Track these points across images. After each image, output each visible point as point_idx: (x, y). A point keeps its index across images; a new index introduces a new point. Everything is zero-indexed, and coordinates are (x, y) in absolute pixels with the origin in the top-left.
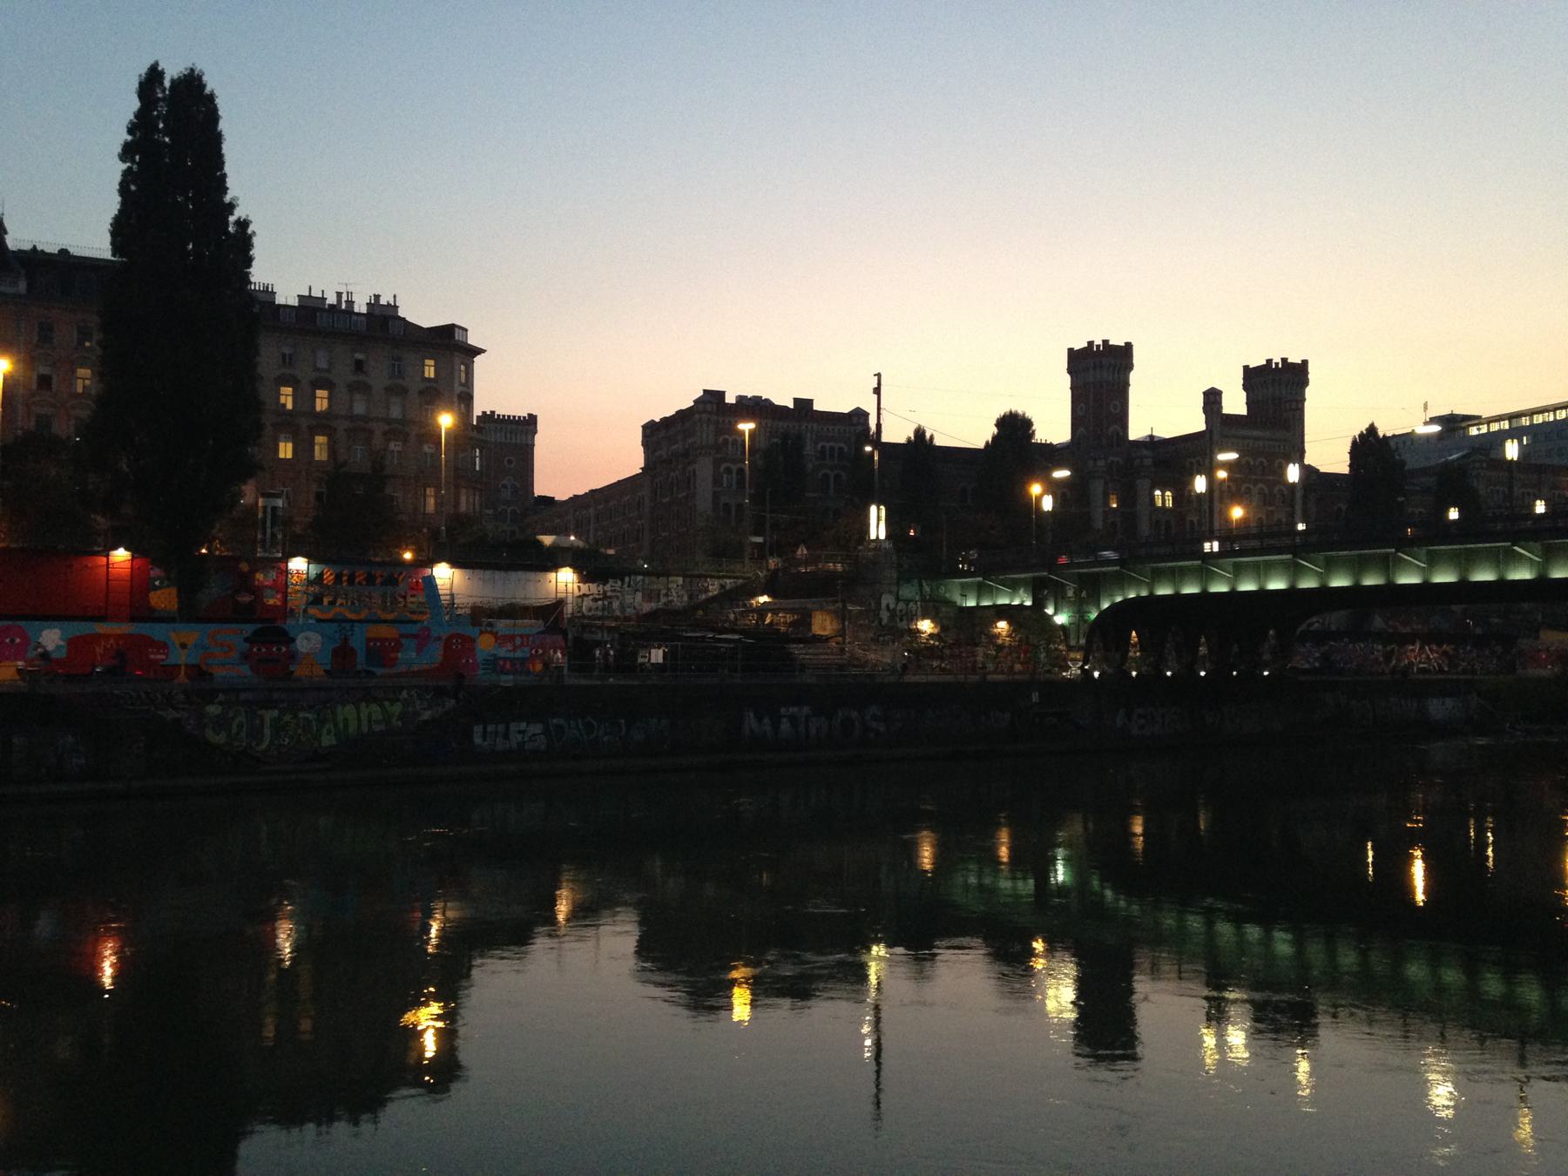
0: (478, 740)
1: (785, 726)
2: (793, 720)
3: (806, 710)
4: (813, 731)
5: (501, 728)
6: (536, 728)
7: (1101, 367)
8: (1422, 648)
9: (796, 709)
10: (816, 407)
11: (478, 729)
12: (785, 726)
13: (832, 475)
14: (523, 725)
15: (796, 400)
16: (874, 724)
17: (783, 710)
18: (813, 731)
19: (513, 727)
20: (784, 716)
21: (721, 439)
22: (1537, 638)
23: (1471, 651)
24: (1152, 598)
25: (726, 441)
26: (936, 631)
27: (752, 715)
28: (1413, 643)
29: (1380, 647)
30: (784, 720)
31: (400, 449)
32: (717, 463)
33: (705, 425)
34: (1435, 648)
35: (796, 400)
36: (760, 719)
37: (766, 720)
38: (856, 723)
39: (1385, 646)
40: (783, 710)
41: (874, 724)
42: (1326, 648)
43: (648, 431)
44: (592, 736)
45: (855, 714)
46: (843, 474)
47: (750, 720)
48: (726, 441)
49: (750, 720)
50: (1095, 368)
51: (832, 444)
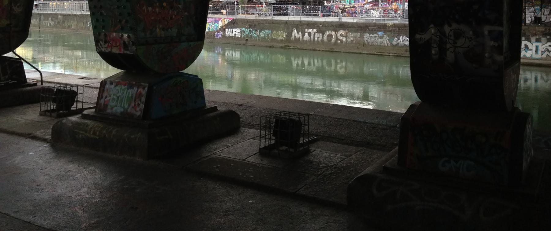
0: (226, 33)
1: (307, 35)
2: (310, 34)
3: (315, 30)
4: (316, 39)
5: (232, 30)
6: (239, 31)
9: (311, 30)
11: (227, 30)
12: (307, 35)
14: (236, 30)
16: (341, 38)
17: (306, 30)
18: (316, 39)
19: (234, 30)
20: (306, 32)
27: (296, 30)
30: (306, 34)
36: (298, 33)
37: (300, 33)
38: (333, 37)
40: (306, 30)
41: (341, 38)
44: (251, 34)
45: (333, 33)
47: (295, 31)
49: (295, 31)
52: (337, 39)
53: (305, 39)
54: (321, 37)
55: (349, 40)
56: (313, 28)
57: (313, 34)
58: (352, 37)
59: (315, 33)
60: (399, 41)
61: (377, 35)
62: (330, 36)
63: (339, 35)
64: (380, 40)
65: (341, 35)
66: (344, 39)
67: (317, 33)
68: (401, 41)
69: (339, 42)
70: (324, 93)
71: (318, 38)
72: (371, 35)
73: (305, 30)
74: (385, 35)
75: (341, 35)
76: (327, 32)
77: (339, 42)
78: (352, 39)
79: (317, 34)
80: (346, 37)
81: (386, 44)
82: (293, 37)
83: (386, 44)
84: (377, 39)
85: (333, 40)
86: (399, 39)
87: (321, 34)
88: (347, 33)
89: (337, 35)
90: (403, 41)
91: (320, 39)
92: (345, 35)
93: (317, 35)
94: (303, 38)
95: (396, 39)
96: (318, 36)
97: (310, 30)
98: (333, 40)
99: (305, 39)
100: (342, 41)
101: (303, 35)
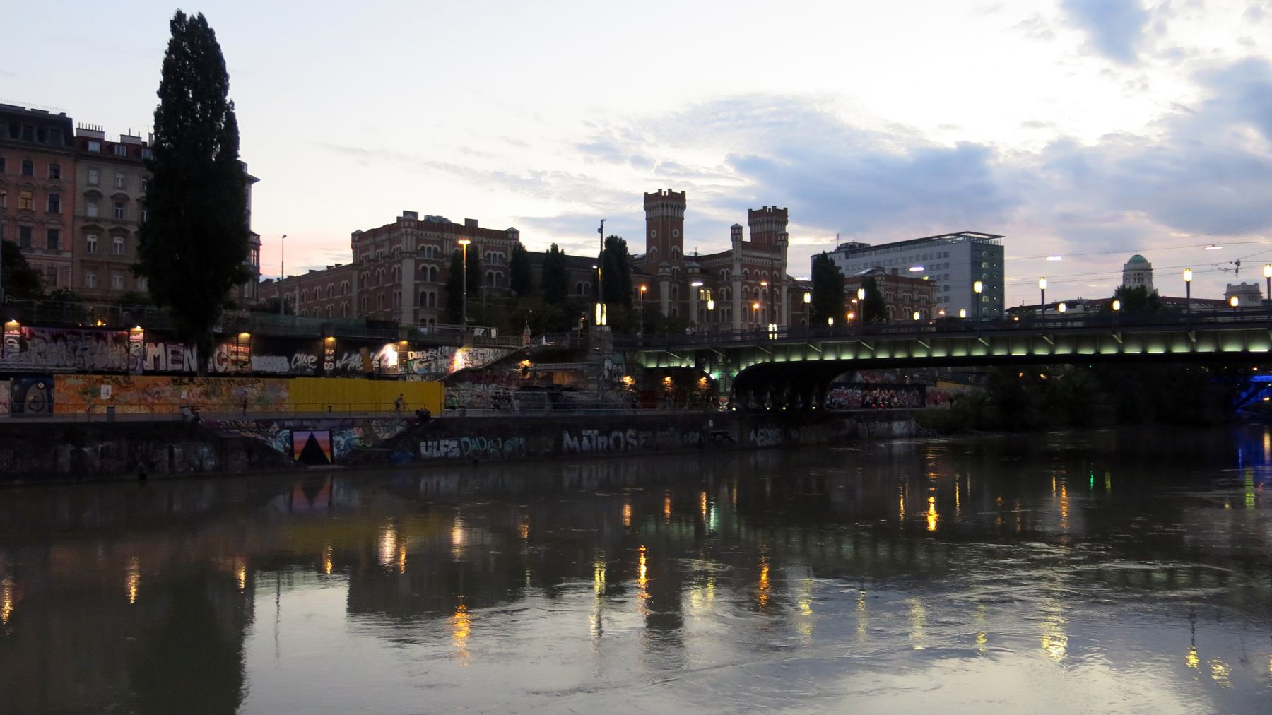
0: (423, 451)
1: (585, 441)
5: (436, 443)
6: (454, 444)
7: (667, 207)
8: (880, 392)
9: (591, 432)
10: (480, 225)
11: (423, 444)
12: (585, 441)
13: (495, 273)
14: (447, 442)
15: (466, 220)
18: (600, 445)
19: (442, 443)
21: (419, 248)
22: (936, 386)
23: (904, 394)
24: (774, 365)
25: (423, 248)
26: (633, 383)
27: (567, 434)
28: (876, 390)
29: (860, 392)
30: (585, 438)
31: (122, 242)
32: (417, 263)
33: (409, 237)
34: (887, 392)
35: (466, 220)
36: (572, 438)
37: (576, 439)
38: (622, 440)
39: (862, 391)
40: (584, 433)
42: (833, 392)
43: (357, 238)
44: (484, 449)
45: (621, 434)
46: (501, 272)
47: (567, 436)
48: (423, 248)
49: (567, 436)
50: (663, 206)
51: (495, 252)
52: (627, 443)
54: (606, 441)
55: (641, 443)
56: (592, 428)
57: (594, 438)
58: (643, 438)
62: (617, 440)
63: (628, 436)
65: (631, 436)
66: (635, 443)
71: (602, 444)
72: (663, 433)
75: (631, 436)
76: (613, 433)
78: (643, 441)
80: (637, 438)
82: (565, 446)
85: (622, 445)
86: (688, 436)
89: (625, 435)
91: (605, 446)
93: (600, 439)
96: (602, 441)
97: (590, 432)
100: (632, 445)
101: (580, 442)
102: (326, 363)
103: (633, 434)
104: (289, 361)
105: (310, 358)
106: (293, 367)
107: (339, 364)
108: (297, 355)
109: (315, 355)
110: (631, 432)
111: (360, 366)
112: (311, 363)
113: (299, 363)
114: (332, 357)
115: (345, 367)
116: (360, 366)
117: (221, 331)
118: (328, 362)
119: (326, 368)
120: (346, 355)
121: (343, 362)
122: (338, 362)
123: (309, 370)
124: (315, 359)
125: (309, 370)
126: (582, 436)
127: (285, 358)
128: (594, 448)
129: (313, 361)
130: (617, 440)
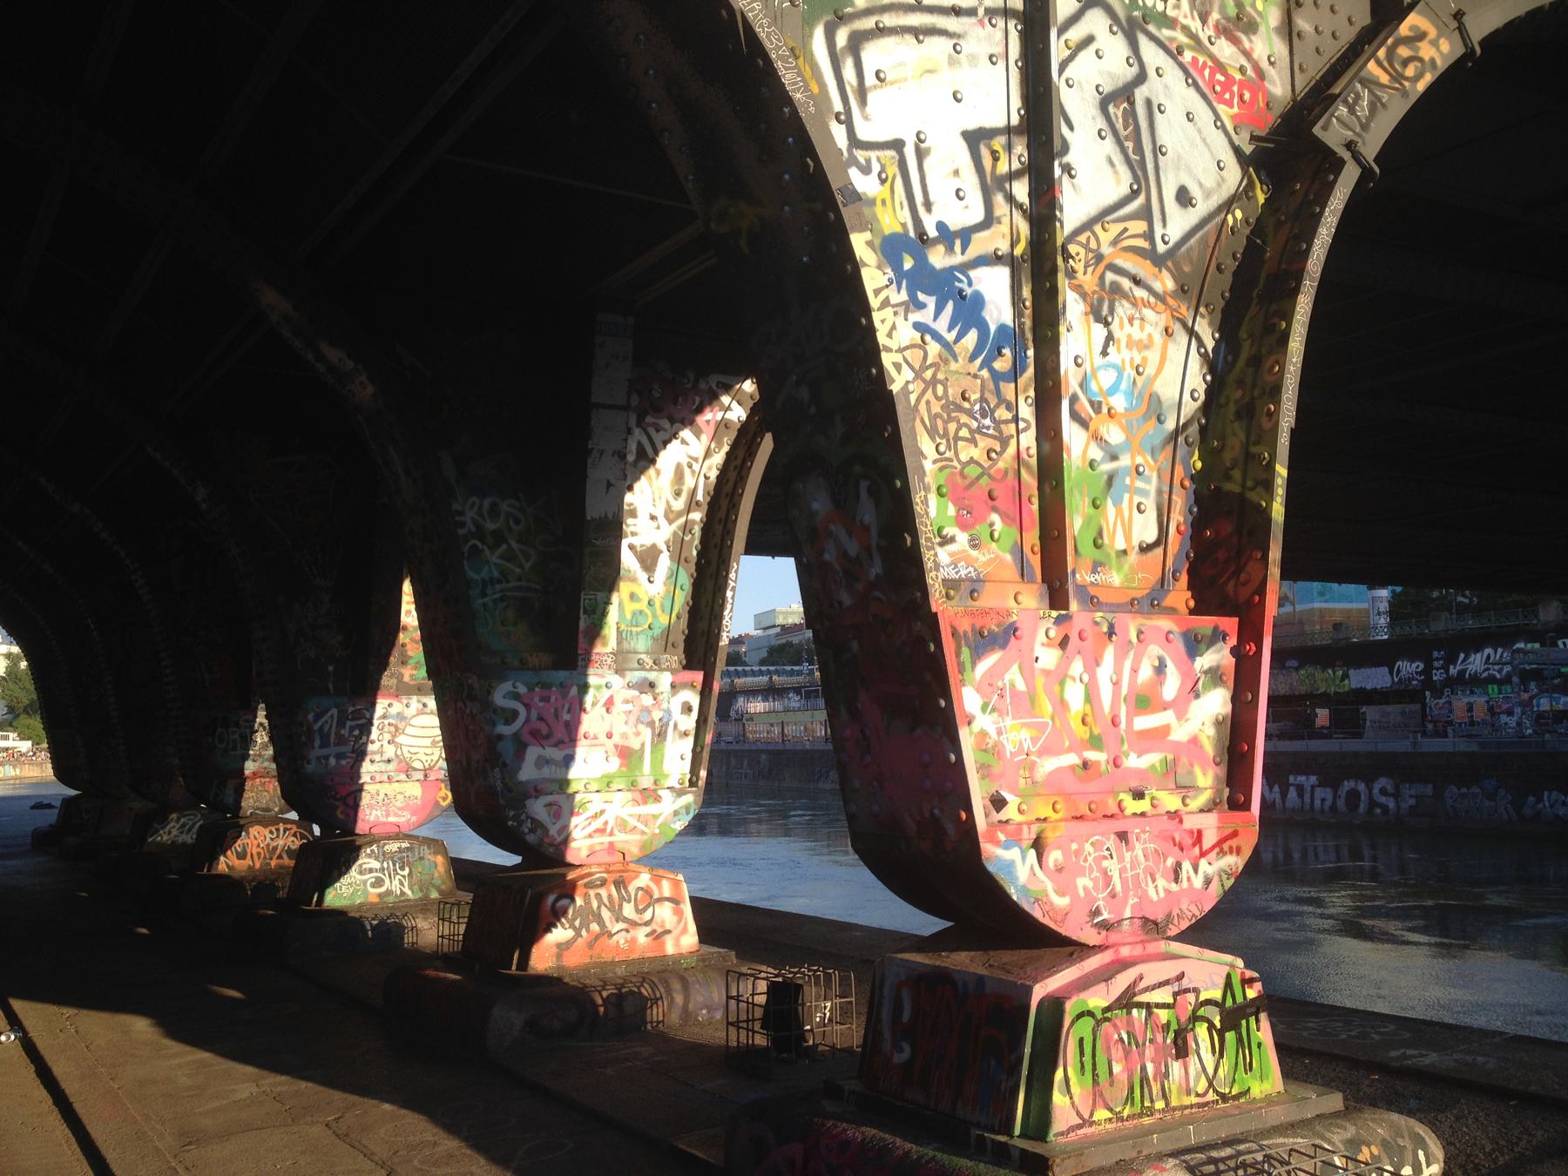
1: (1292, 793)
2: (1300, 789)
3: (1313, 779)
12: (1292, 793)
16: (1383, 799)
18: (1317, 803)
20: (1292, 785)
30: (1292, 789)
37: (1276, 788)
38: (1363, 797)
40: (1291, 779)
41: (1383, 799)
45: (1362, 787)
52: (1373, 804)
53: (1289, 805)
54: (1330, 798)
55: (1404, 806)
56: (1307, 773)
57: (1309, 789)
58: (1411, 796)
59: (1313, 787)
60: (1540, 806)
61: (1478, 790)
62: (1353, 795)
63: (1376, 791)
64: (1487, 803)
65: (1383, 792)
66: (1391, 804)
67: (1318, 786)
68: (1547, 804)
69: (1378, 811)
70: (1190, 1036)
71: (1323, 800)
72: (1464, 790)
73: (1288, 780)
74: (1500, 790)
76: (1346, 783)
77: (1378, 811)
78: (1412, 802)
79: (1318, 789)
80: (1396, 796)
81: (1505, 816)
83: (1505, 816)
84: (1478, 801)
85: (1363, 807)
86: (1540, 799)
87: (1328, 790)
88: (1397, 787)
89: (1370, 790)
90: (1551, 806)
91: (1328, 803)
92: (1392, 791)
93: (1319, 793)
94: (1284, 803)
95: (1531, 798)
96: (1323, 795)
97: (1301, 779)
98: (1363, 807)
99: (1289, 805)
100: (1385, 809)
101: (1284, 795)
102: (1434, 671)
103: (1390, 788)
104: (1391, 673)
105: (1414, 665)
106: (1396, 680)
107: (1453, 671)
108: (1399, 663)
109: (1421, 661)
110: (1383, 782)
111: (1484, 671)
112: (1417, 673)
113: (1402, 674)
114: (1441, 662)
115: (1462, 673)
116: (1484, 671)
117: (1386, 637)
118: (1437, 669)
119: (1435, 678)
120: (1462, 656)
121: (1458, 668)
122: (1452, 667)
123: (1414, 682)
124: (1422, 666)
125: (1414, 682)
126: (1289, 785)
127: (1385, 670)
128: (1307, 807)
129: (1419, 670)
130: (1353, 795)
